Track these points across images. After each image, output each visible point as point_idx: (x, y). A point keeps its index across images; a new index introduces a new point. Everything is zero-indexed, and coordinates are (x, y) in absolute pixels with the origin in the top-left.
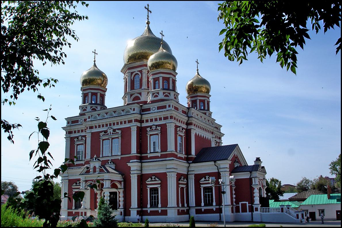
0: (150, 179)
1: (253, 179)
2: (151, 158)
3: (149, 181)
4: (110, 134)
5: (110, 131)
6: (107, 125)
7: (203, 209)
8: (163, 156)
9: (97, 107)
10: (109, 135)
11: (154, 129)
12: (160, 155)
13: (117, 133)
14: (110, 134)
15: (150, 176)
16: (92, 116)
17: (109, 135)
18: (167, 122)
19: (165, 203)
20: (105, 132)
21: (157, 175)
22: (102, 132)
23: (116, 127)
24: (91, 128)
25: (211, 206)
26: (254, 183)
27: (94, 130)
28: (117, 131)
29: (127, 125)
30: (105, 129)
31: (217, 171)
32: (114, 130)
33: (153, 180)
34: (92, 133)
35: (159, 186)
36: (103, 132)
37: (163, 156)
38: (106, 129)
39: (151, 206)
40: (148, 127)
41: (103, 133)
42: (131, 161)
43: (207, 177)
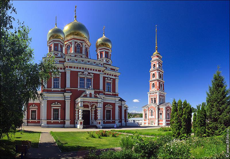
0: (107, 105)
2: (54, 91)
4: (86, 75)
6: (83, 68)
7: (52, 121)
8: (113, 95)
9: (58, 53)
14: (86, 75)
15: (108, 103)
16: (70, 59)
19: (64, 118)
20: (83, 72)
21: (110, 104)
22: (80, 72)
23: (90, 71)
24: (71, 67)
27: (73, 69)
28: (91, 74)
30: (82, 71)
32: (89, 73)
34: (71, 71)
40: (106, 77)
41: (81, 73)
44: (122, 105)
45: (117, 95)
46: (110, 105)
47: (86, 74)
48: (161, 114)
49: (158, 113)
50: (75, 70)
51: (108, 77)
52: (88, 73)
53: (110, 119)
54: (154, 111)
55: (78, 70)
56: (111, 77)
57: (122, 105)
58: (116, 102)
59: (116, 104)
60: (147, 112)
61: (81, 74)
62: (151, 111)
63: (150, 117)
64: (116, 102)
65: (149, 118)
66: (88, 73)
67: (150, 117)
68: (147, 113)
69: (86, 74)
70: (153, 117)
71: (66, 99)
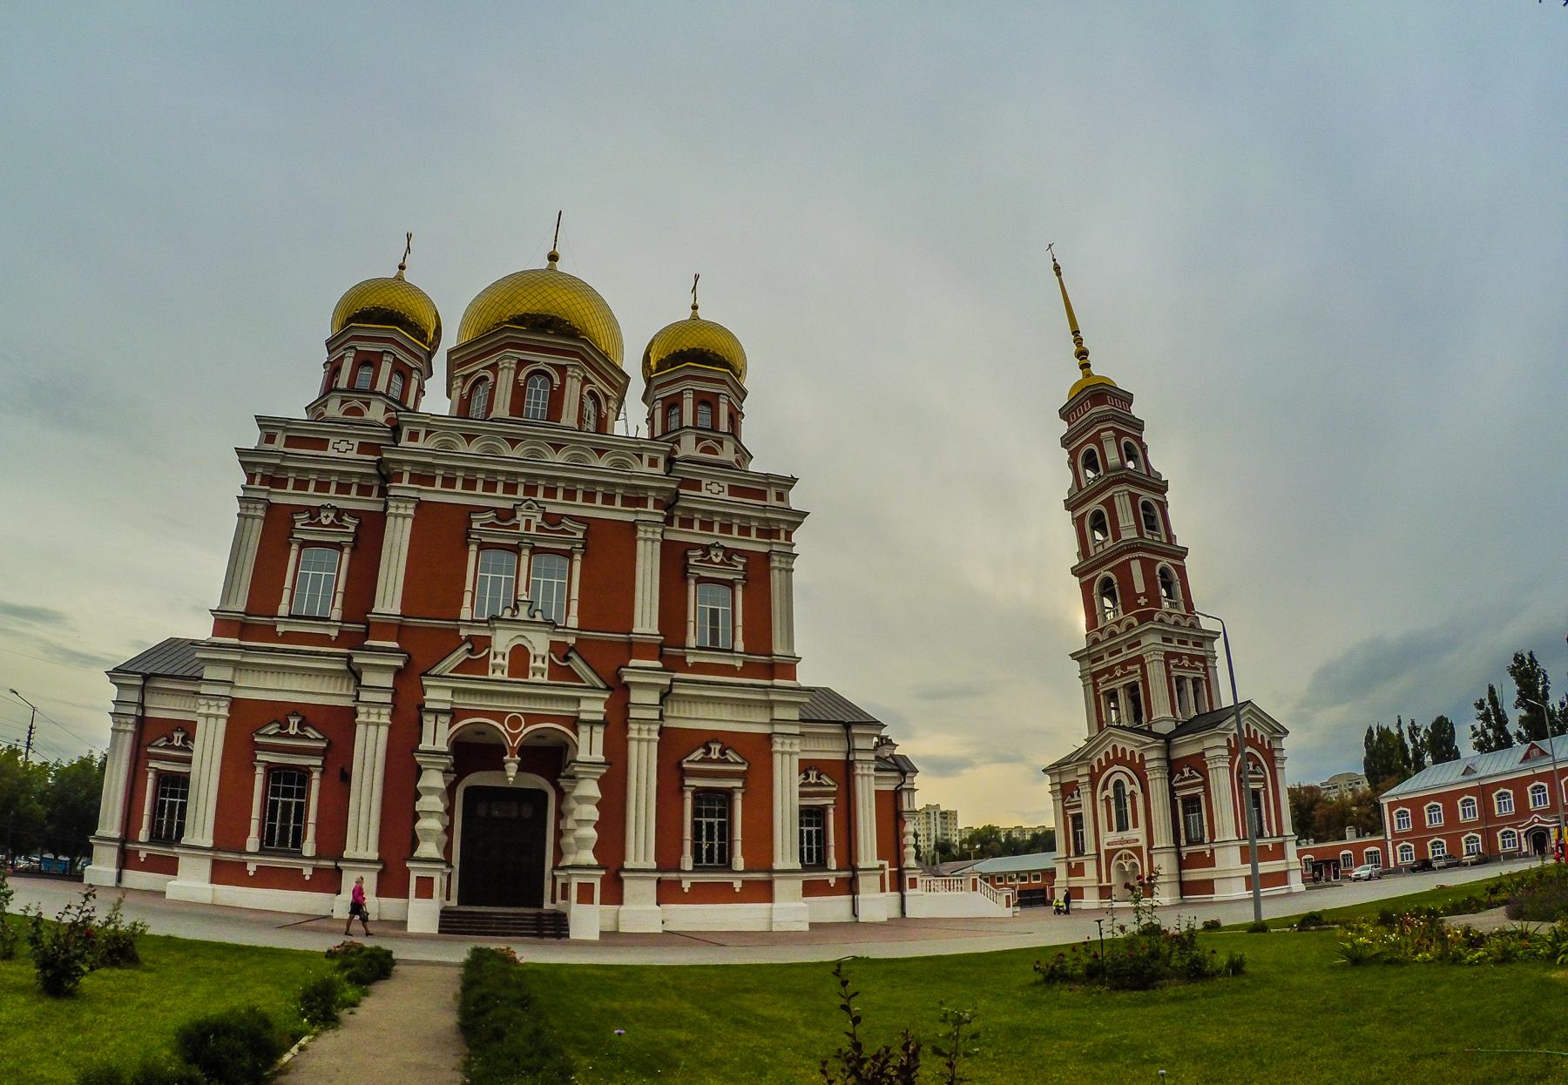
0: (698, 754)
1: (905, 796)
3: (693, 761)
4: (528, 527)
5: (529, 520)
10: (522, 529)
11: (717, 560)
12: (739, 664)
13: (564, 531)
14: (528, 527)
17: (522, 529)
18: (775, 548)
20: (506, 515)
21: (728, 740)
22: (487, 509)
25: (823, 871)
26: (906, 808)
27: (435, 494)
29: (618, 513)
31: (841, 757)
33: (715, 757)
35: (739, 784)
36: (491, 514)
37: (749, 669)
38: (509, 505)
39: (267, 846)
42: (633, 663)
43: (813, 774)
44: (859, 756)
45: (788, 668)
46: (722, 752)
47: (528, 522)
48: (1192, 804)
49: (1172, 795)
50: (457, 497)
51: (706, 549)
52: (546, 516)
53: (726, 864)
54: (1138, 789)
55: (478, 496)
56: (734, 541)
57: (859, 756)
58: (778, 728)
59: (778, 740)
60: (1086, 800)
61: (492, 525)
62: (1110, 792)
63: (1109, 838)
64: (778, 728)
65: (1104, 847)
66: (546, 516)
67: (1109, 838)
68: (1086, 811)
69: (528, 522)
70: (1137, 834)
71: (364, 696)
